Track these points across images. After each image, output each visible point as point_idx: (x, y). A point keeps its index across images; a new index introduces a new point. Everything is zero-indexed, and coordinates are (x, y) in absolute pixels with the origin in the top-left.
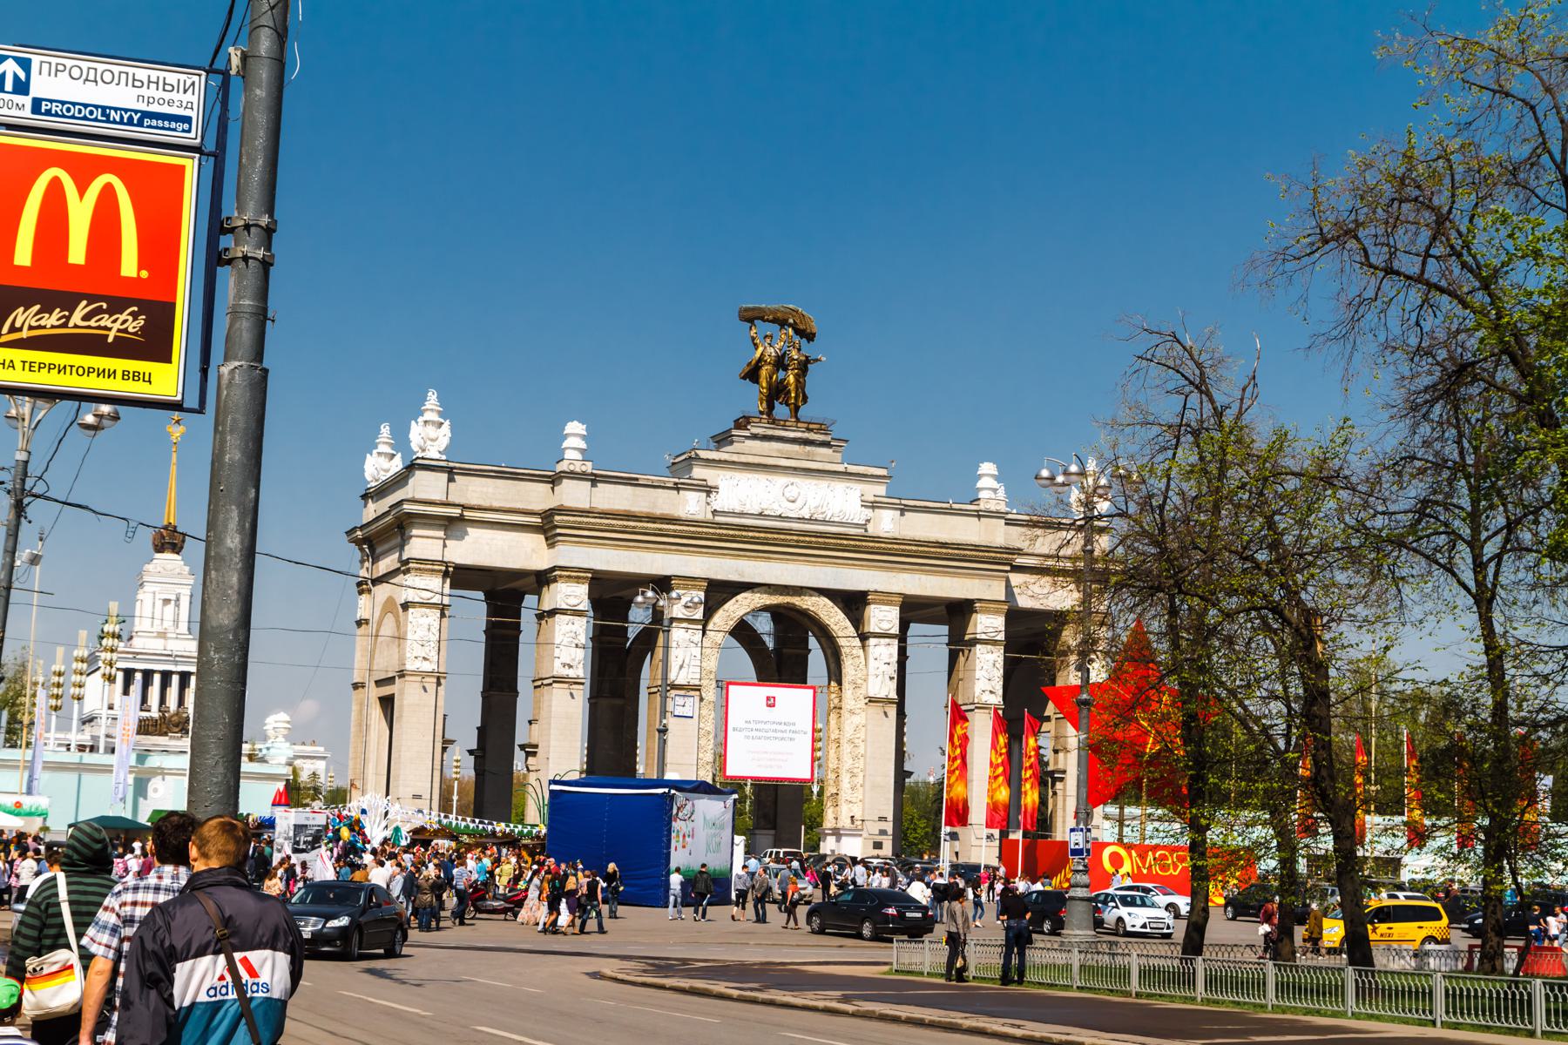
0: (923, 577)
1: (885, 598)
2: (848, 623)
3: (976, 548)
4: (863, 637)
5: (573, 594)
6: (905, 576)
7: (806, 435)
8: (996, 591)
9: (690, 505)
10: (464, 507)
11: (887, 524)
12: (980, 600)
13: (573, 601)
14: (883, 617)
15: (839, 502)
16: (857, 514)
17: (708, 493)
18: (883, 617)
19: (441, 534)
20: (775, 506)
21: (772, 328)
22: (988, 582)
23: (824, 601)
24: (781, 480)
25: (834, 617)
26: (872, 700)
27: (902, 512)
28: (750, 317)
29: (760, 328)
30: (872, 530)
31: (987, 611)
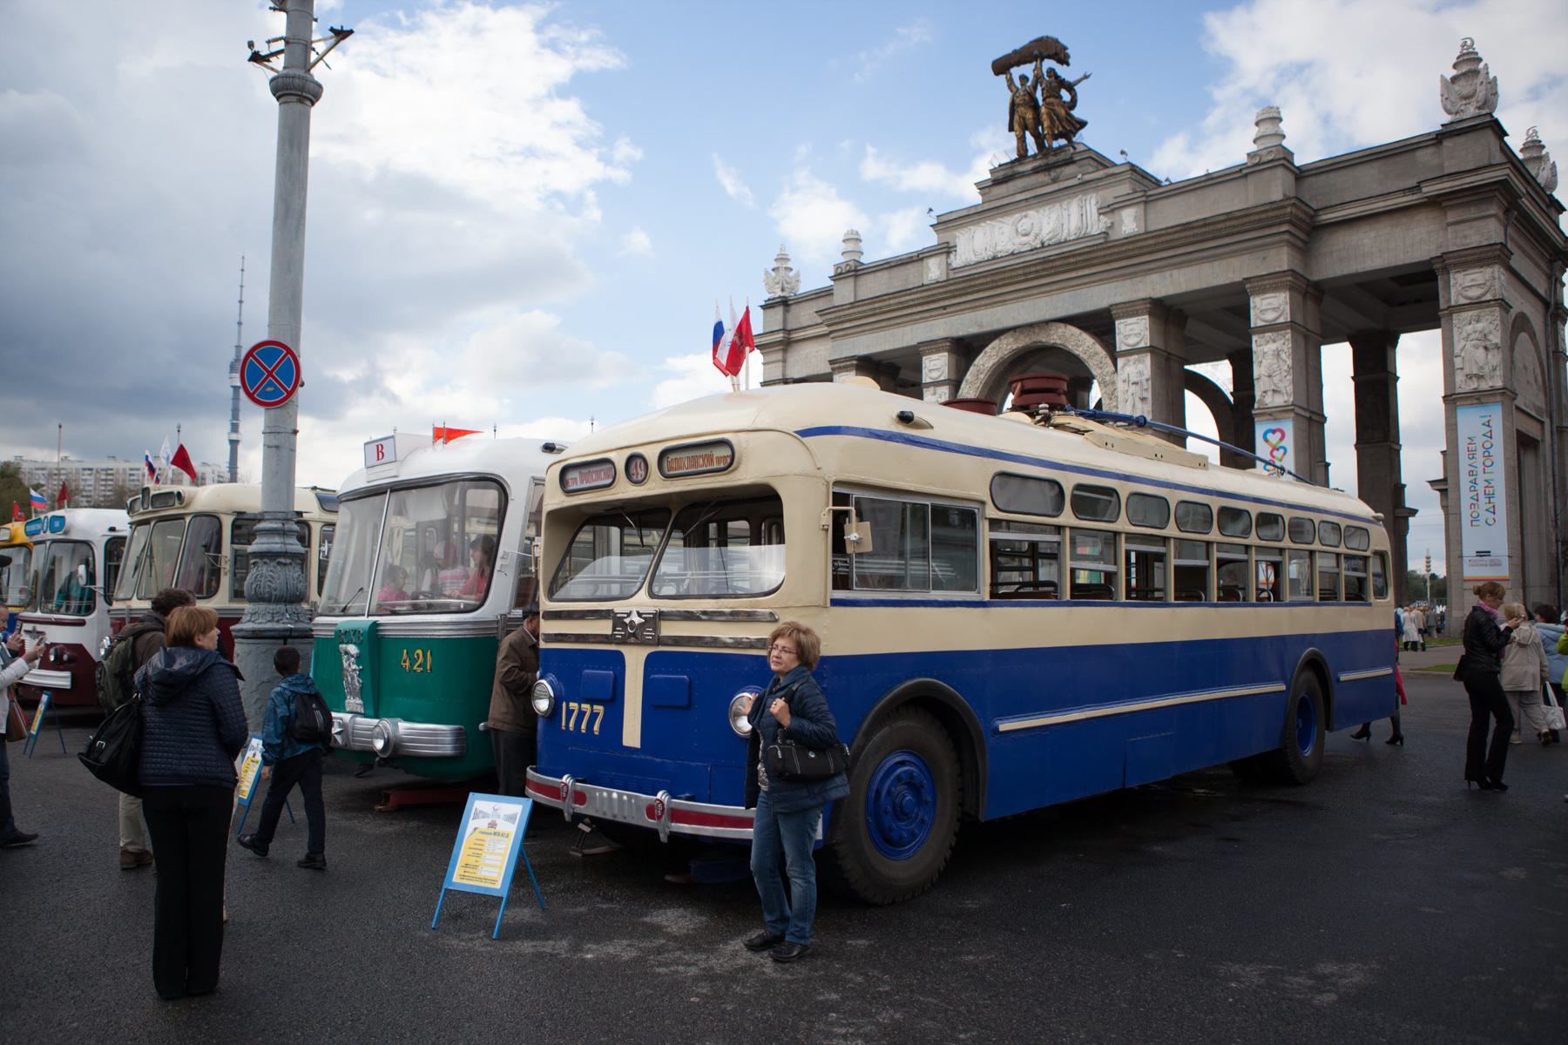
0: (1175, 272)
1: (1130, 309)
2: (1098, 348)
3: (1229, 216)
4: (1114, 355)
6: (1155, 277)
9: (934, 271)
11: (1129, 223)
14: (1134, 331)
16: (1096, 225)
17: (948, 253)
18: (1134, 331)
19: (779, 356)
22: (1261, 254)
24: (1009, 220)
25: (1083, 345)
27: (1146, 202)
29: (1016, 72)
30: (1114, 236)
31: (1262, 291)
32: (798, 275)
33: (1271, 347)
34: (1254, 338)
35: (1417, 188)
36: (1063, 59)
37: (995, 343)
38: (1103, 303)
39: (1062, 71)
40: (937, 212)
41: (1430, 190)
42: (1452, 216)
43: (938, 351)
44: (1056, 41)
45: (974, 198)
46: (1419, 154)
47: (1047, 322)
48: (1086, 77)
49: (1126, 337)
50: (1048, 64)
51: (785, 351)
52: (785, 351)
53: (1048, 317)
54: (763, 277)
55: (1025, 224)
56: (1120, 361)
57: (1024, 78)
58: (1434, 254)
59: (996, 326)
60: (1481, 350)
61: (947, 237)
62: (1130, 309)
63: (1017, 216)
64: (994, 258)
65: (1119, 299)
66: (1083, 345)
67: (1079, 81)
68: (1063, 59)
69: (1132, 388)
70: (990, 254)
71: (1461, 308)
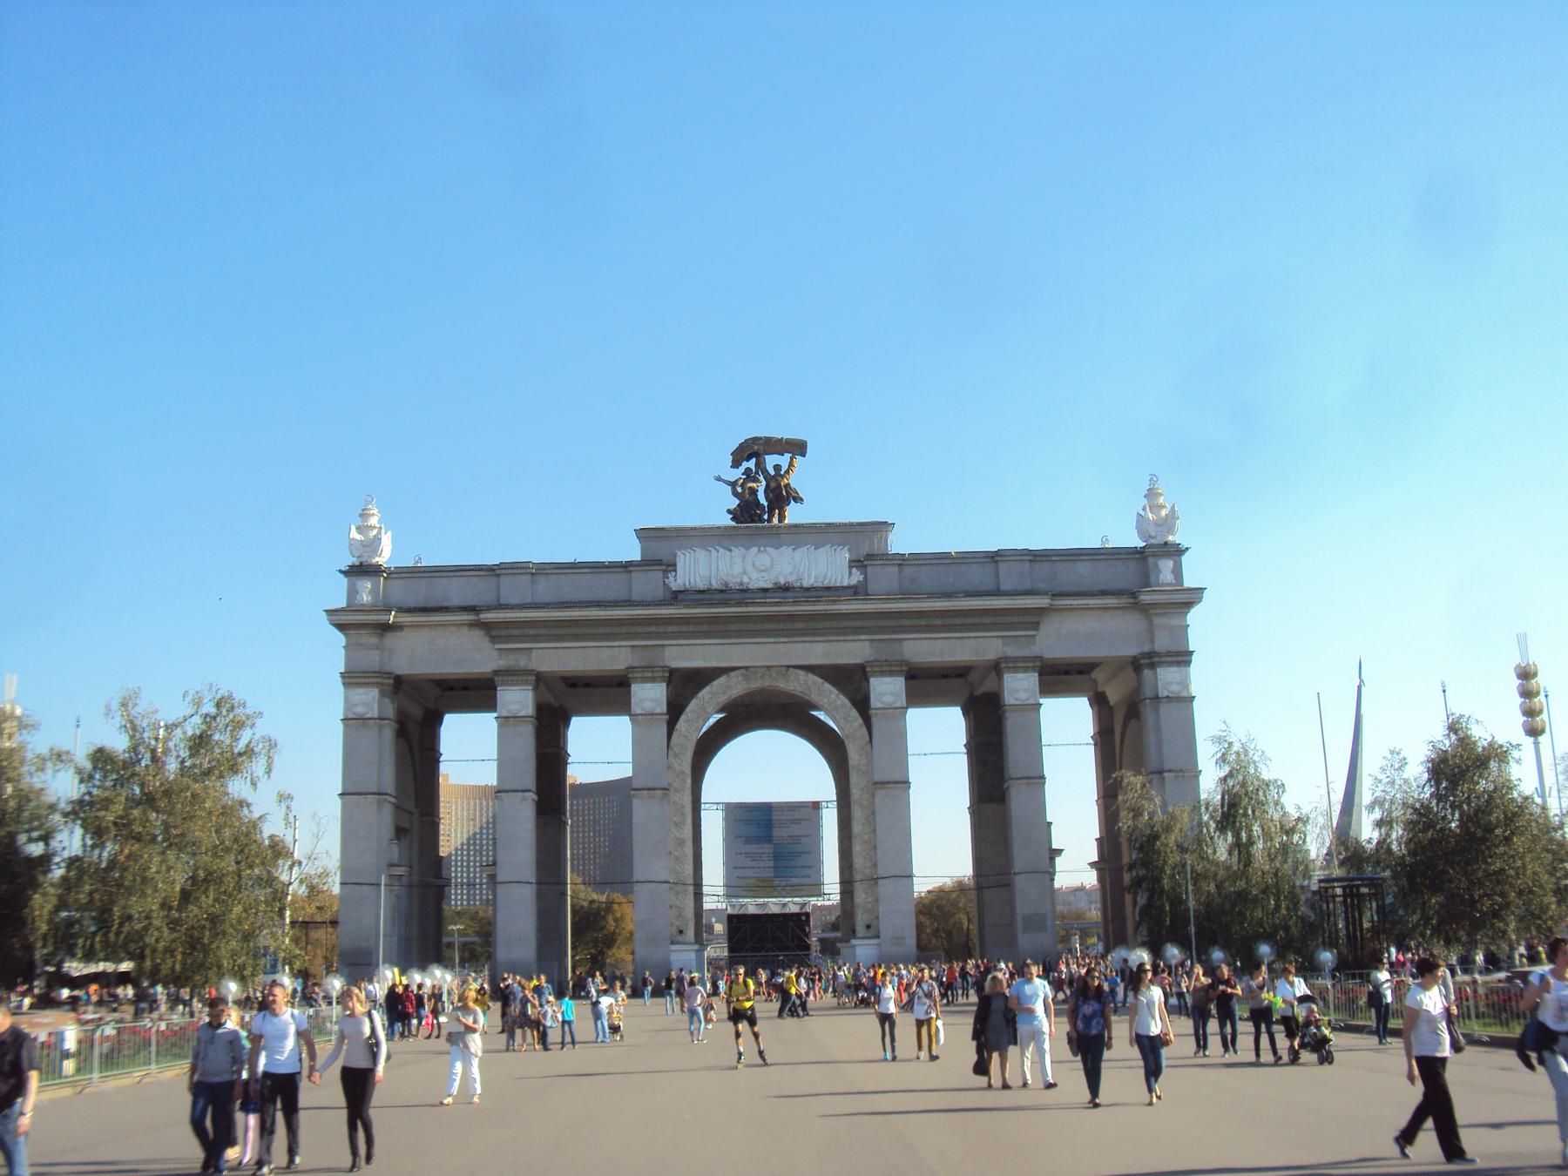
5: (519, 699)
9: (646, 585)
12: (1006, 659)
18: (886, 690)
20: (746, 580)
23: (813, 678)
37: (723, 679)
43: (653, 680)
61: (661, 550)
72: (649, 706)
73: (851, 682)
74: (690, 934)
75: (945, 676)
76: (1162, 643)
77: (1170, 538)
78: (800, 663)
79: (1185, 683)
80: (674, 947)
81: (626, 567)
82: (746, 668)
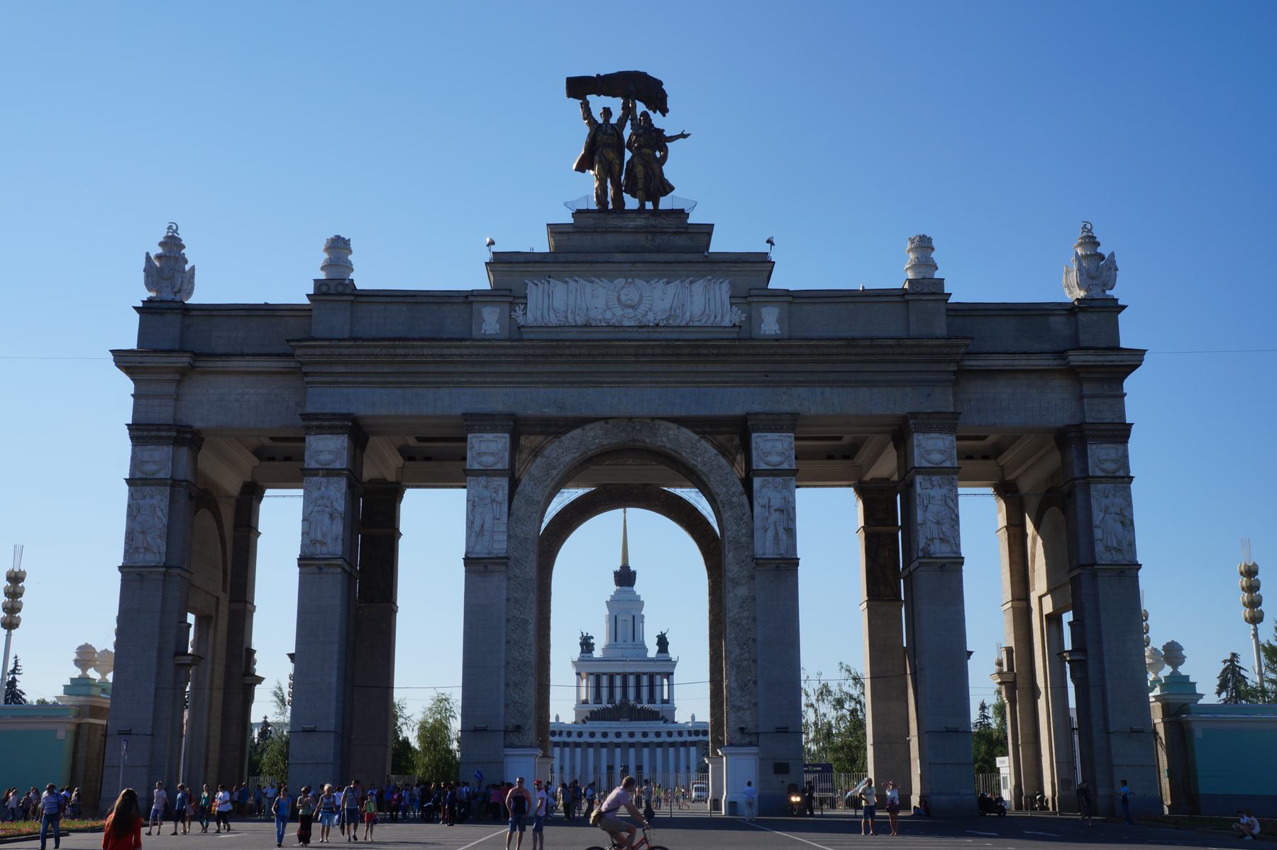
0: (827, 390)
6: (802, 391)
7: (652, 222)
8: (942, 400)
10: (197, 355)
11: (770, 322)
12: (914, 415)
13: (325, 457)
15: (702, 304)
18: (772, 448)
20: (608, 315)
21: (616, 105)
23: (687, 434)
26: (758, 562)
28: (579, 87)
29: (597, 103)
31: (928, 429)
32: (193, 268)
33: (937, 493)
34: (918, 479)
35: (1060, 354)
36: (664, 111)
37: (576, 433)
38: (739, 411)
39: (657, 120)
40: (495, 248)
41: (1076, 358)
42: (1088, 389)
43: (494, 429)
44: (660, 83)
45: (542, 244)
46: (1051, 319)
47: (653, 419)
48: (683, 136)
49: (767, 454)
50: (641, 107)
51: (179, 382)
52: (179, 382)
53: (660, 414)
54: (143, 265)
55: (631, 292)
56: (757, 482)
57: (607, 112)
58: (1068, 422)
59: (586, 412)
60: (1119, 525)
62: (775, 423)
63: (621, 281)
64: (585, 326)
65: (757, 408)
66: (704, 453)
67: (672, 139)
68: (664, 111)
69: (775, 516)
70: (580, 321)
71: (1098, 479)
72: (488, 460)
73: (735, 434)
74: (531, 735)
75: (830, 457)
76: (1097, 413)
77: (1108, 292)
78: (668, 414)
79: (1124, 461)
80: (508, 751)
81: (468, 299)
82: (606, 419)
